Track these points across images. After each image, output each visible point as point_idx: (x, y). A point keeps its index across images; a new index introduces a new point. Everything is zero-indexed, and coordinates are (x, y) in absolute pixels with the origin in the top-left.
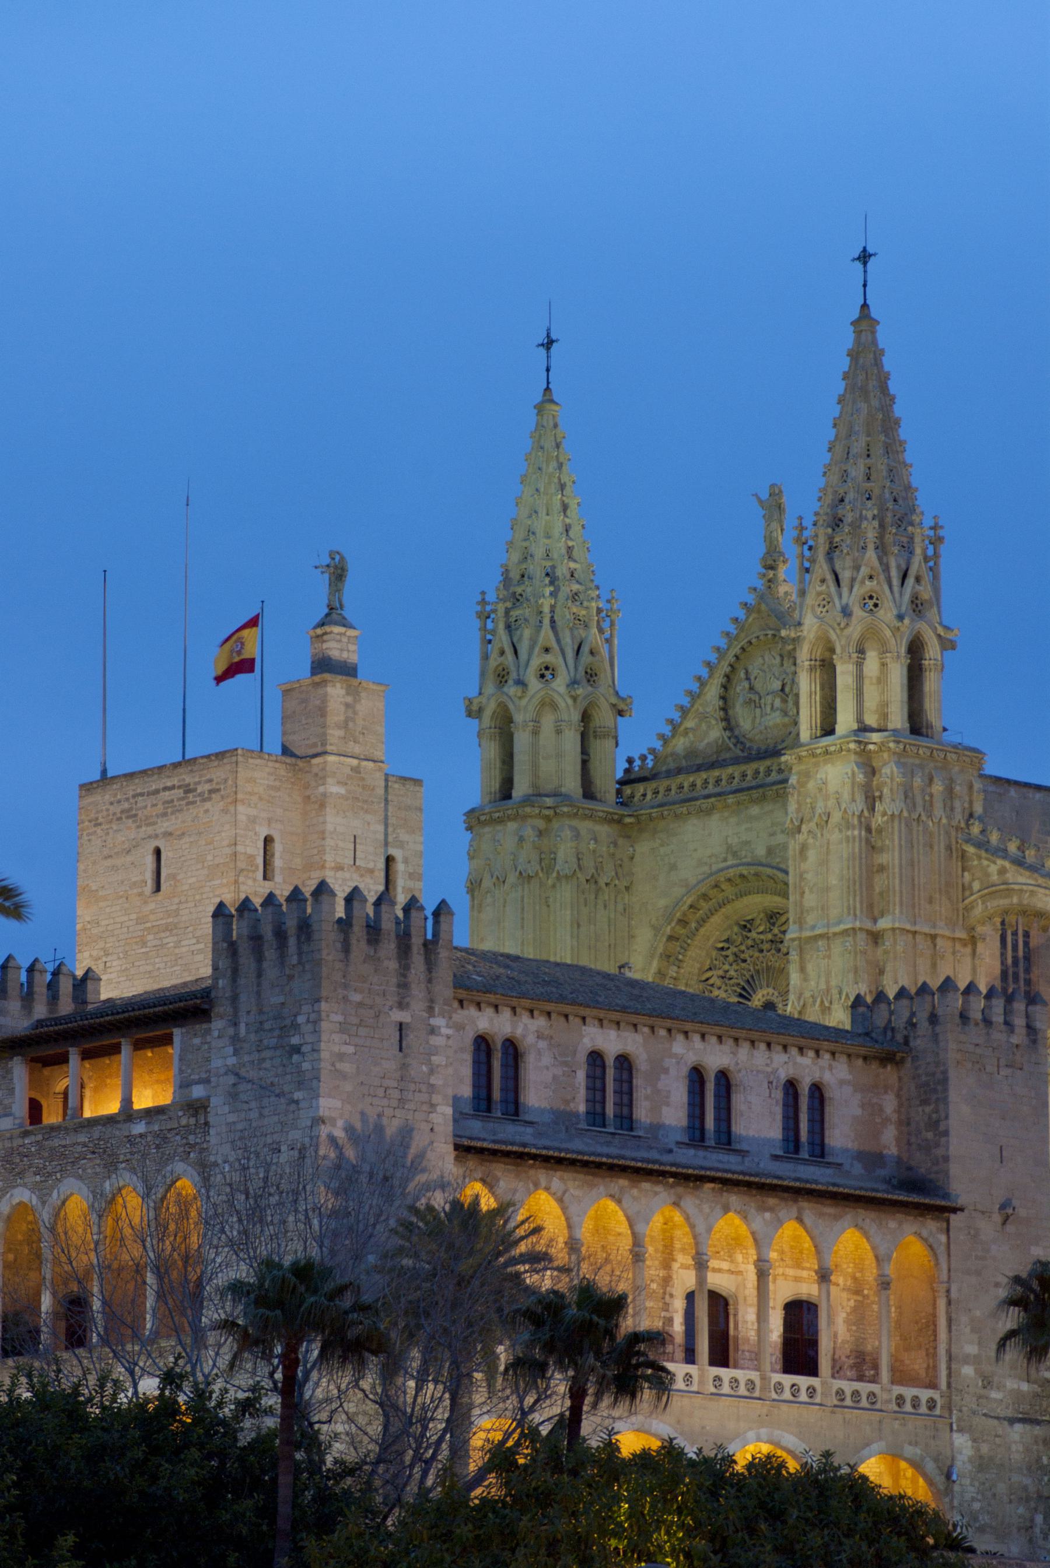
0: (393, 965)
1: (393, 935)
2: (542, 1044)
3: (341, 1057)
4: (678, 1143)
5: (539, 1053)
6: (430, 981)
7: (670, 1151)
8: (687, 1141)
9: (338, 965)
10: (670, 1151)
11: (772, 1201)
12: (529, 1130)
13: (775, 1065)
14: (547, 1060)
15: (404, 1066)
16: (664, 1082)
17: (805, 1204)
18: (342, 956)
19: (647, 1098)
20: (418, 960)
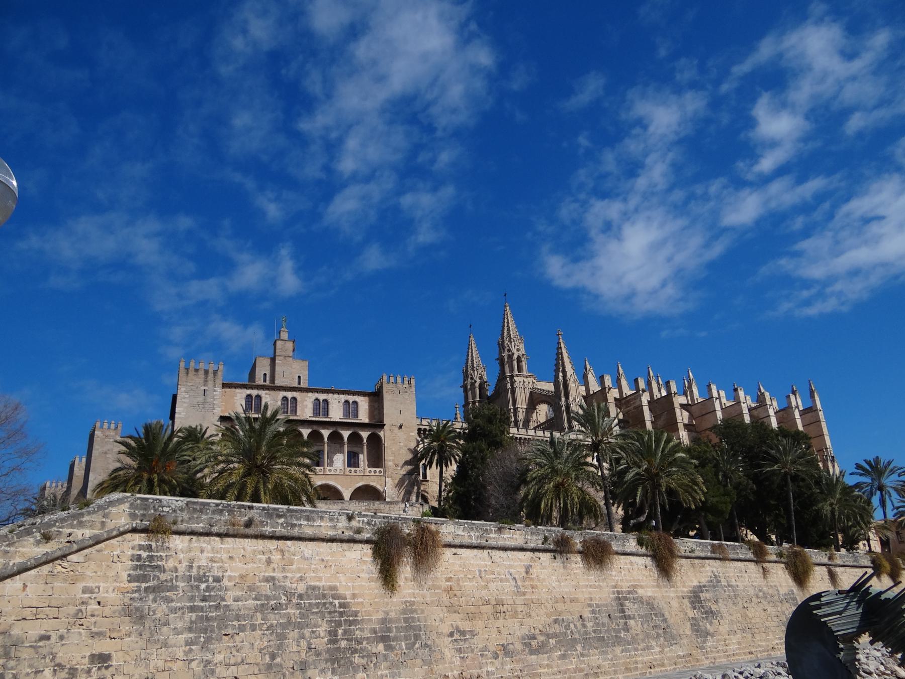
3: (184, 398)
16: (305, 403)
20: (211, 375)
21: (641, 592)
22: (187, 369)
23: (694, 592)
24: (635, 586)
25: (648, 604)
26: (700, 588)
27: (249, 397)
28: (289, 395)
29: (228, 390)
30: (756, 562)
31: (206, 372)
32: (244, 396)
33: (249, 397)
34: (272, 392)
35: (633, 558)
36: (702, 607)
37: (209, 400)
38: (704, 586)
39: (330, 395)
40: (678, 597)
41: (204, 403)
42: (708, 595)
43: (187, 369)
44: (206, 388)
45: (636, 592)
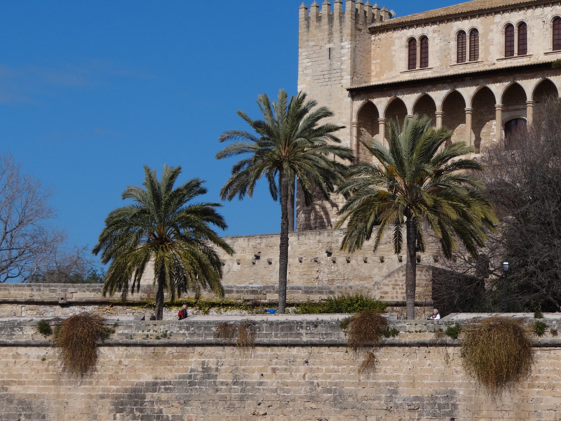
0: (327, 27)
1: (326, 16)
2: (435, 35)
3: (306, 68)
4: (497, 60)
5: (434, 38)
6: (341, 29)
7: (494, 64)
8: (504, 57)
9: (306, 33)
10: (494, 64)
11: (500, 78)
12: (430, 71)
13: (545, 13)
14: (437, 41)
15: (331, 65)
17: (517, 75)
18: (306, 30)
19: (482, 45)
20: (336, 22)
21: (14, 389)
22: (307, 19)
23: (134, 390)
24: (9, 383)
25: (21, 402)
26: (153, 386)
27: (412, 41)
28: (466, 25)
29: (383, 36)
30: (354, 345)
31: (331, 18)
32: (404, 42)
33: (412, 41)
34: (443, 26)
35: (22, 350)
36: (141, 411)
37: (336, 65)
38: (165, 383)
39: (530, 11)
40: (91, 397)
41: (331, 70)
42: (164, 396)
43: (307, 19)
44: (331, 45)
45: (6, 389)
